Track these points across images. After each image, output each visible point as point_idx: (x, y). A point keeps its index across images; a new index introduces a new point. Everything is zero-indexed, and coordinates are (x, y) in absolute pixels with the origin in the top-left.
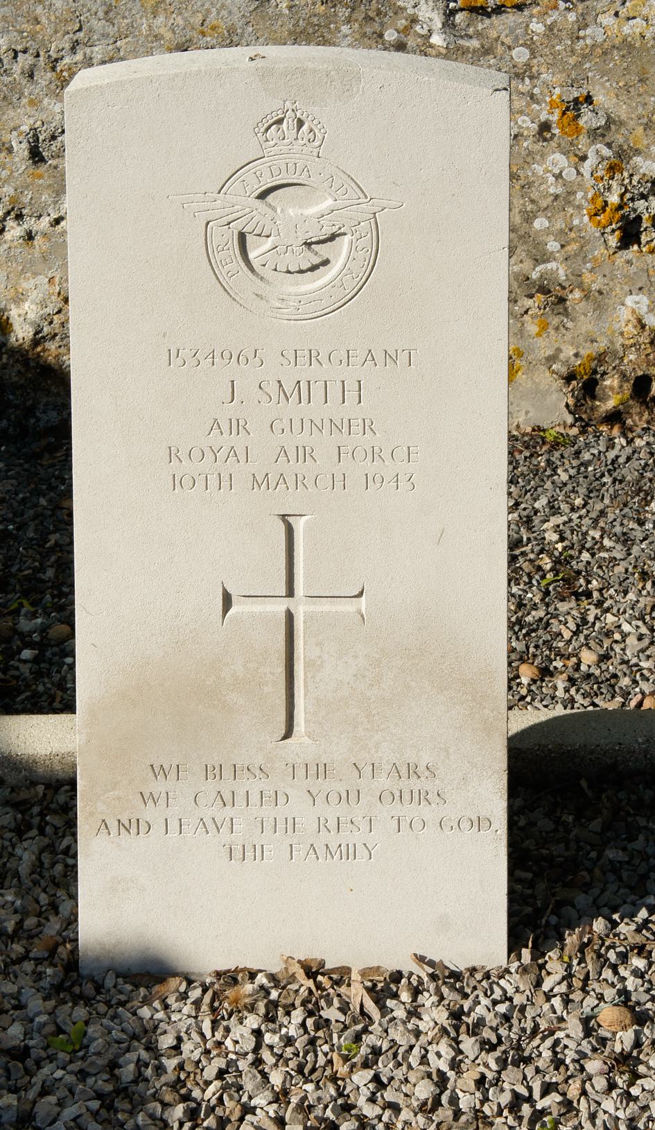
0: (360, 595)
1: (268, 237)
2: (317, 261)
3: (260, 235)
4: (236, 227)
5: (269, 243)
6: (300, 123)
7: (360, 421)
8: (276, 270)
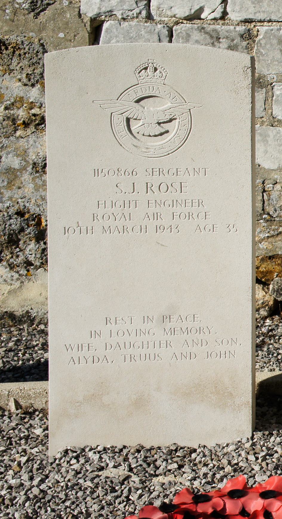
1: (140, 120)
2: (163, 131)
3: (135, 119)
5: (141, 123)
6: (156, 69)
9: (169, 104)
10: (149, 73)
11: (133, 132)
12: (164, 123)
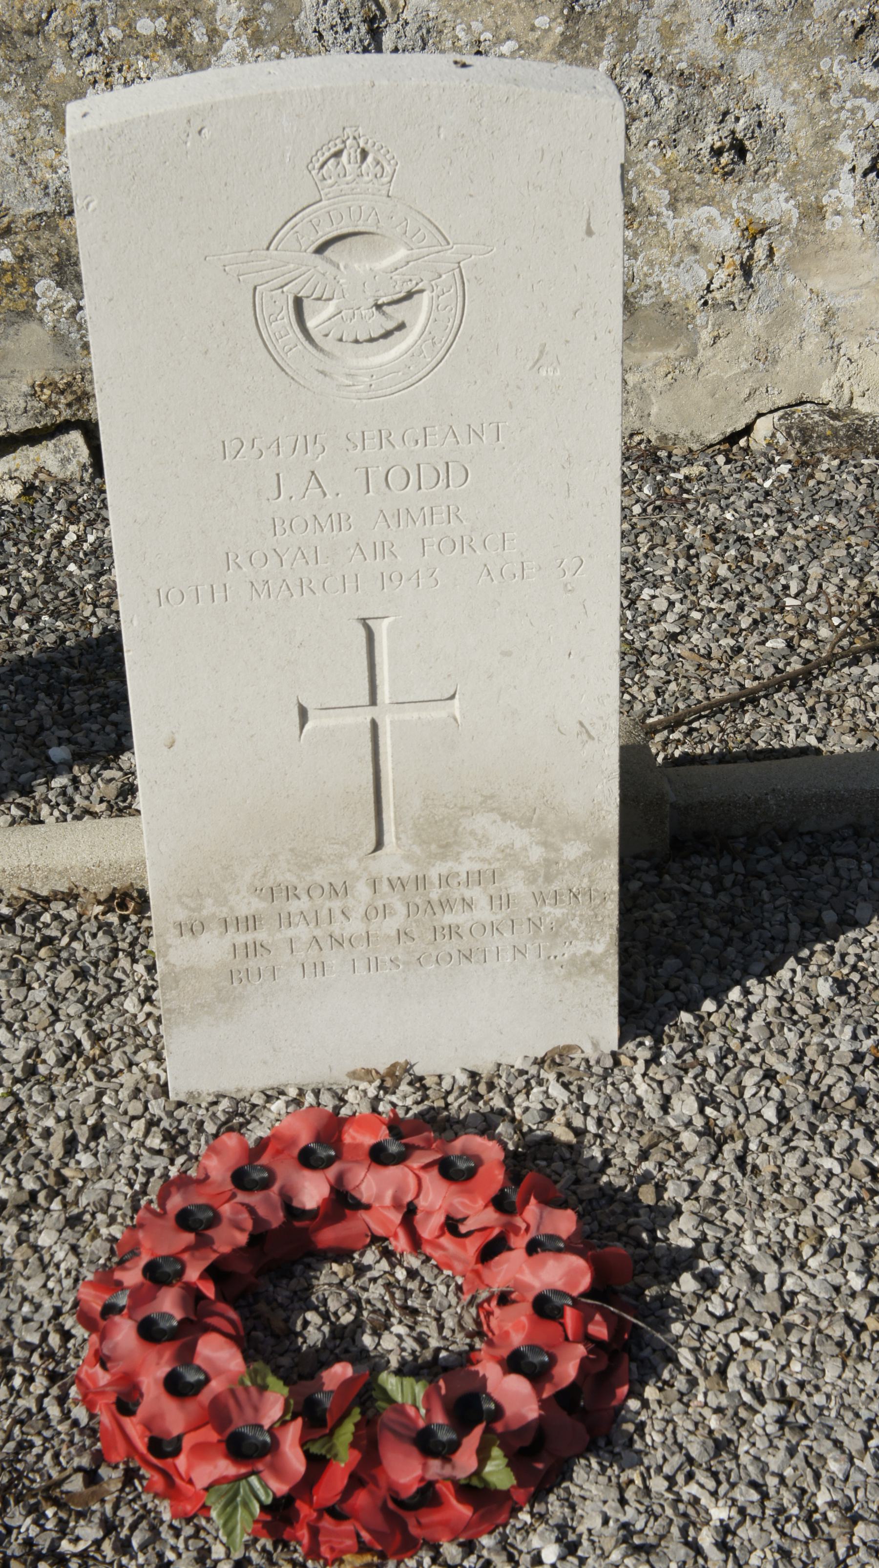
1: (329, 299)
2: (390, 325)
3: (319, 299)
4: (291, 290)
6: (364, 154)
7: (444, 508)
8: (341, 340)
9: (401, 253)
10: (348, 167)
11: (313, 333)
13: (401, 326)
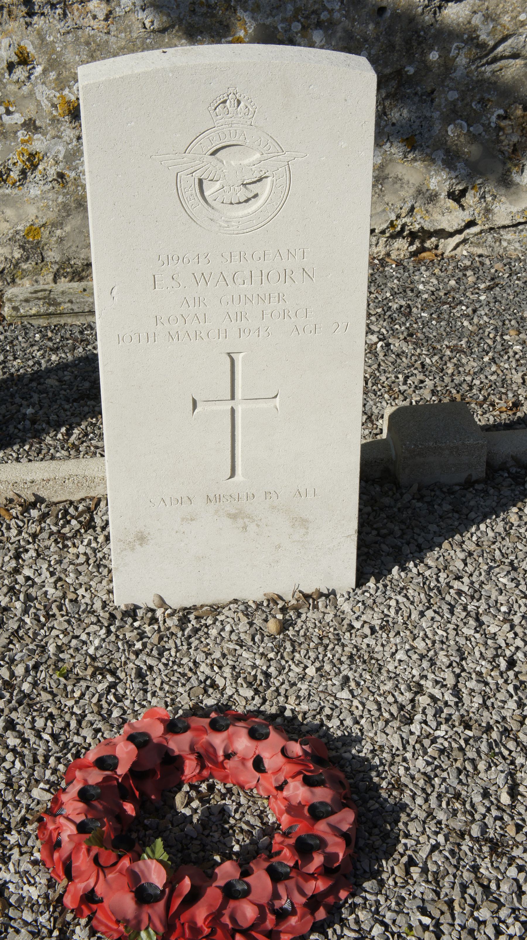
0: (276, 397)
2: (251, 195)
4: (197, 175)
5: (218, 185)
6: (239, 102)
9: (257, 156)
10: (230, 109)
11: (208, 199)
12: (250, 184)
13: (256, 196)
